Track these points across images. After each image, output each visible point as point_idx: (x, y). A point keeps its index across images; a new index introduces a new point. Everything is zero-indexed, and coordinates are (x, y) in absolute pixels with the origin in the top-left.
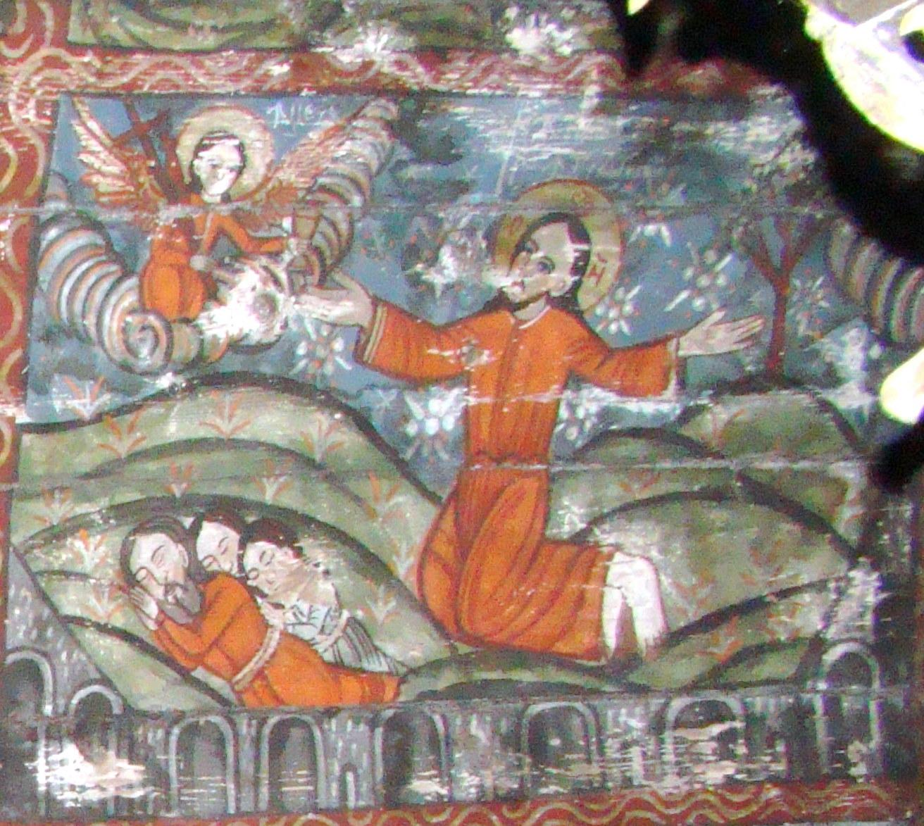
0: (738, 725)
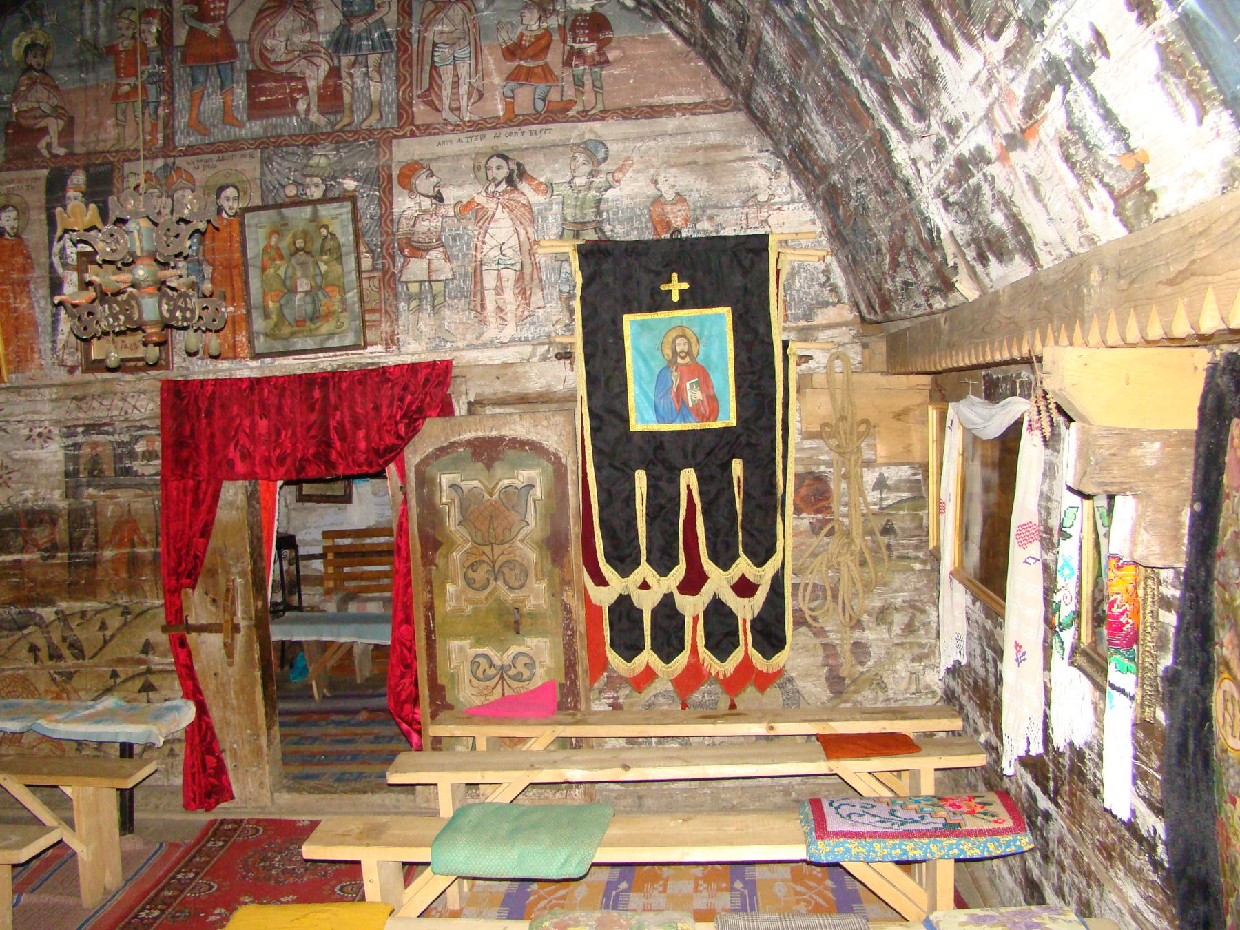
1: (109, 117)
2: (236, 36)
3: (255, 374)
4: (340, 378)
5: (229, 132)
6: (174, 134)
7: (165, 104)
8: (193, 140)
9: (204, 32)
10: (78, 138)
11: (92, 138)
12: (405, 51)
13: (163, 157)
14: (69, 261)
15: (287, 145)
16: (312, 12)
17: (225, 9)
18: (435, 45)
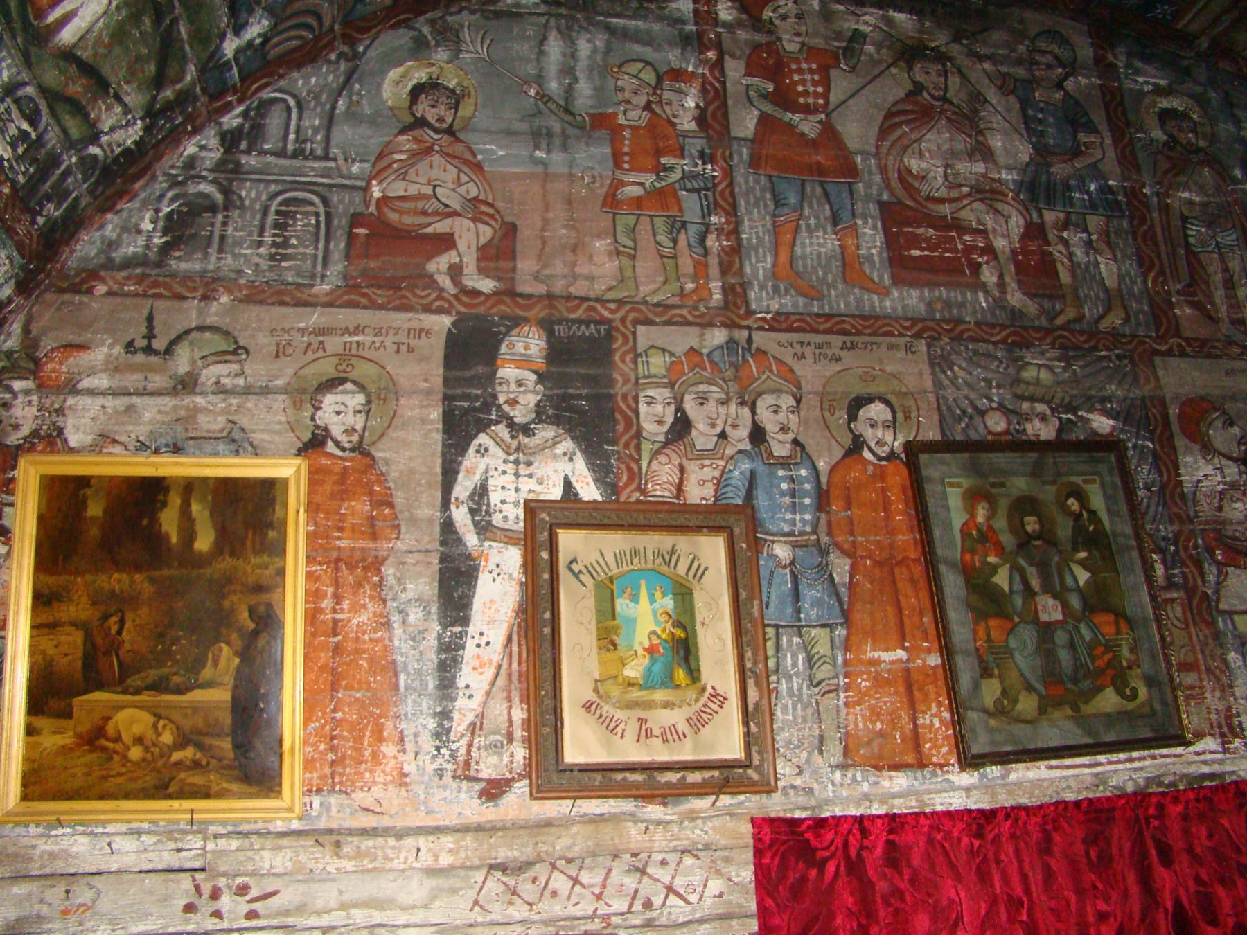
0: (33, 136)
1: (599, 236)
2: (852, 143)
3: (978, 802)
4: (1161, 807)
5: (859, 301)
6: (745, 286)
7: (720, 231)
8: (787, 302)
9: (790, 127)
10: (526, 265)
11: (559, 268)
12: (1143, 220)
13: (724, 325)
14: (497, 520)
15: (973, 339)
16: (980, 132)
17: (826, 96)
18: (1184, 219)
